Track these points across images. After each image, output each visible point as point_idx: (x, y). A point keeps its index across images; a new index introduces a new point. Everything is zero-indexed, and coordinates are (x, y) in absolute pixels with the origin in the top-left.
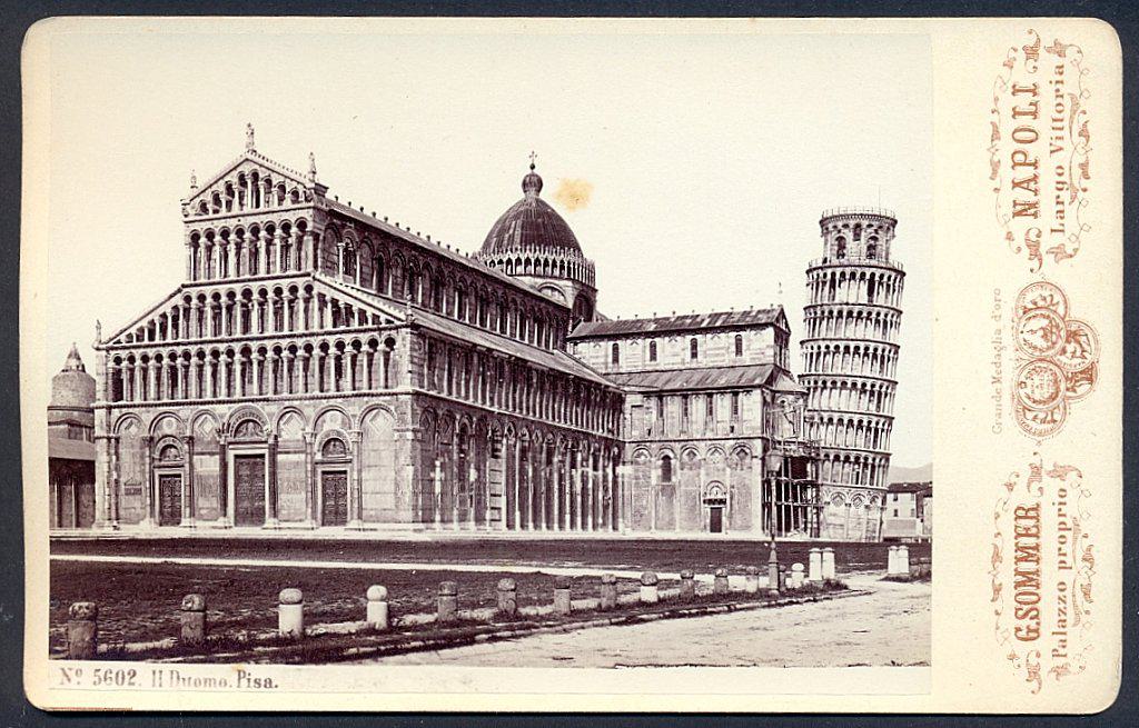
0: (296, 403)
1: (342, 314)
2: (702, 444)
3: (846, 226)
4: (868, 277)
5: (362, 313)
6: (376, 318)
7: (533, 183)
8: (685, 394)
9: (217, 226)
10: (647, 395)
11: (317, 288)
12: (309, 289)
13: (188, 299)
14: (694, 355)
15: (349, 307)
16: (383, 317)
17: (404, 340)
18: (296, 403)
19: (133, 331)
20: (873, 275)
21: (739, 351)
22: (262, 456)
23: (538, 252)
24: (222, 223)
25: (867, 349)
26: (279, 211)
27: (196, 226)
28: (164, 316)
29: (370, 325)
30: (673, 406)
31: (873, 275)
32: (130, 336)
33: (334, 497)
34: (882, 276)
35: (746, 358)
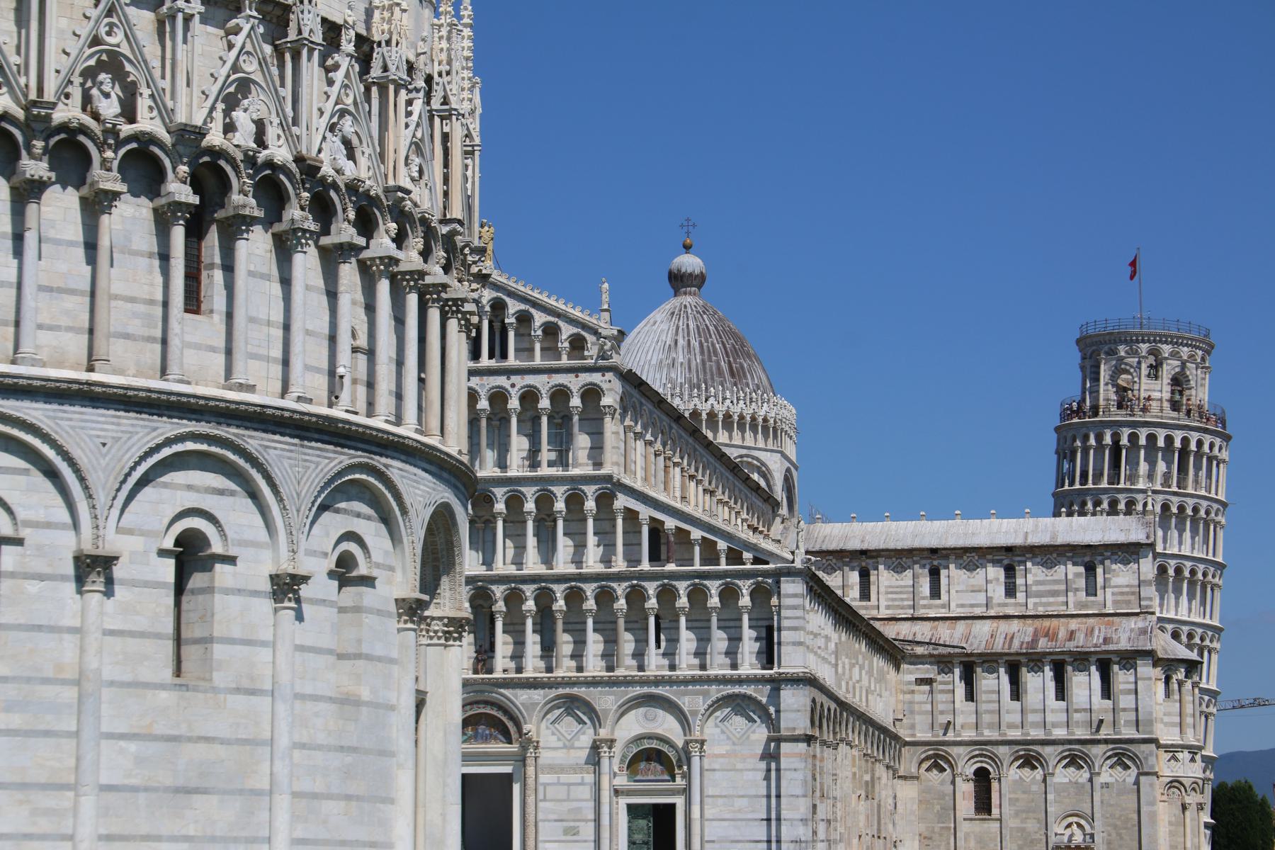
0: (575, 691)
2: (1047, 751)
3: (1134, 353)
4: (1178, 444)
5: (708, 546)
8: (1015, 666)
10: (944, 663)
11: (622, 501)
12: (605, 500)
14: (1011, 591)
15: (682, 534)
16: (747, 556)
18: (575, 691)
20: (1185, 441)
21: (1091, 590)
23: (712, 400)
25: (1178, 571)
29: (723, 566)
30: (993, 683)
31: (1185, 441)
34: (1200, 443)
35: (1108, 600)
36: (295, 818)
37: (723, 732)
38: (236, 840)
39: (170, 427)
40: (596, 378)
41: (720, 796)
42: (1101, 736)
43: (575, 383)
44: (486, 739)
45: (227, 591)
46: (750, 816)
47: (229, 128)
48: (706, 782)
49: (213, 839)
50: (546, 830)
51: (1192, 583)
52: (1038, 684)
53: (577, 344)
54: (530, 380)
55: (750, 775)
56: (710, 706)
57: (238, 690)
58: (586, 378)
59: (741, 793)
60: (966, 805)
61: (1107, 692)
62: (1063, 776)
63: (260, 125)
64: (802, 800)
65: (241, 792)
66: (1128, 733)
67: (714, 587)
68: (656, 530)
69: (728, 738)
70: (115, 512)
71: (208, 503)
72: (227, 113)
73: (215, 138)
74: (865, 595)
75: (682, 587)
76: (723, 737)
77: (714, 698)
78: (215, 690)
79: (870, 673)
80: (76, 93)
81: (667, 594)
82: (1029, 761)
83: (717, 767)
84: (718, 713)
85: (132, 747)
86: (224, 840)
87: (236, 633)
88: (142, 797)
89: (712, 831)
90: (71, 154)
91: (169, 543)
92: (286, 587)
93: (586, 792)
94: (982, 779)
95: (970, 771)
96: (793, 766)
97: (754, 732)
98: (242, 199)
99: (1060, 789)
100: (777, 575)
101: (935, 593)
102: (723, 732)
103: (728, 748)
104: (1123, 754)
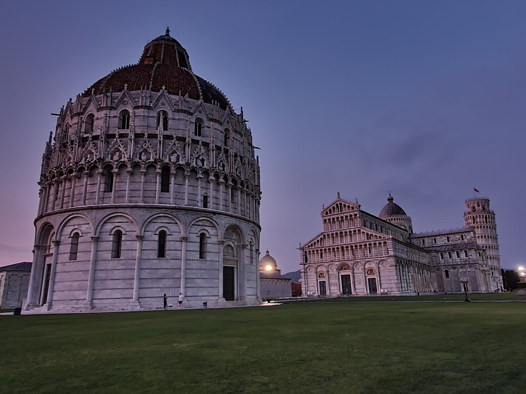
1: (369, 236)
6: (380, 237)
7: (391, 200)
9: (331, 217)
13: (324, 236)
14: (448, 241)
17: (390, 242)
19: (310, 244)
20: (486, 216)
21: (463, 239)
22: (349, 275)
24: (333, 217)
26: (346, 212)
27: (325, 218)
28: (318, 241)
32: (309, 247)
33: (372, 285)
36: (186, 283)
38: (172, 288)
39: (155, 212)
40: (356, 212)
42: (467, 263)
43: (353, 214)
44: (346, 269)
45: (170, 241)
47: (170, 160)
49: (166, 287)
50: (356, 283)
51: (491, 238)
52: (454, 255)
53: (353, 208)
54: (347, 214)
57: (172, 259)
58: (354, 213)
60: (444, 276)
61: (467, 256)
62: (461, 270)
63: (178, 158)
65: (173, 278)
66: (472, 262)
67: (377, 242)
68: (368, 234)
70: (144, 228)
71: (166, 225)
72: (169, 157)
73: (167, 161)
74: (424, 244)
75: (372, 243)
78: (167, 259)
79: (419, 255)
80: (138, 156)
81: (370, 244)
82: (454, 268)
85: (148, 271)
86: (169, 287)
87: (172, 249)
88: (150, 280)
89: (382, 282)
90: (136, 165)
91: (157, 233)
92: (185, 239)
93: (361, 277)
94: (447, 272)
95: (444, 270)
98: (173, 170)
99: (460, 272)
100: (387, 239)
101: (435, 242)
104: (471, 265)
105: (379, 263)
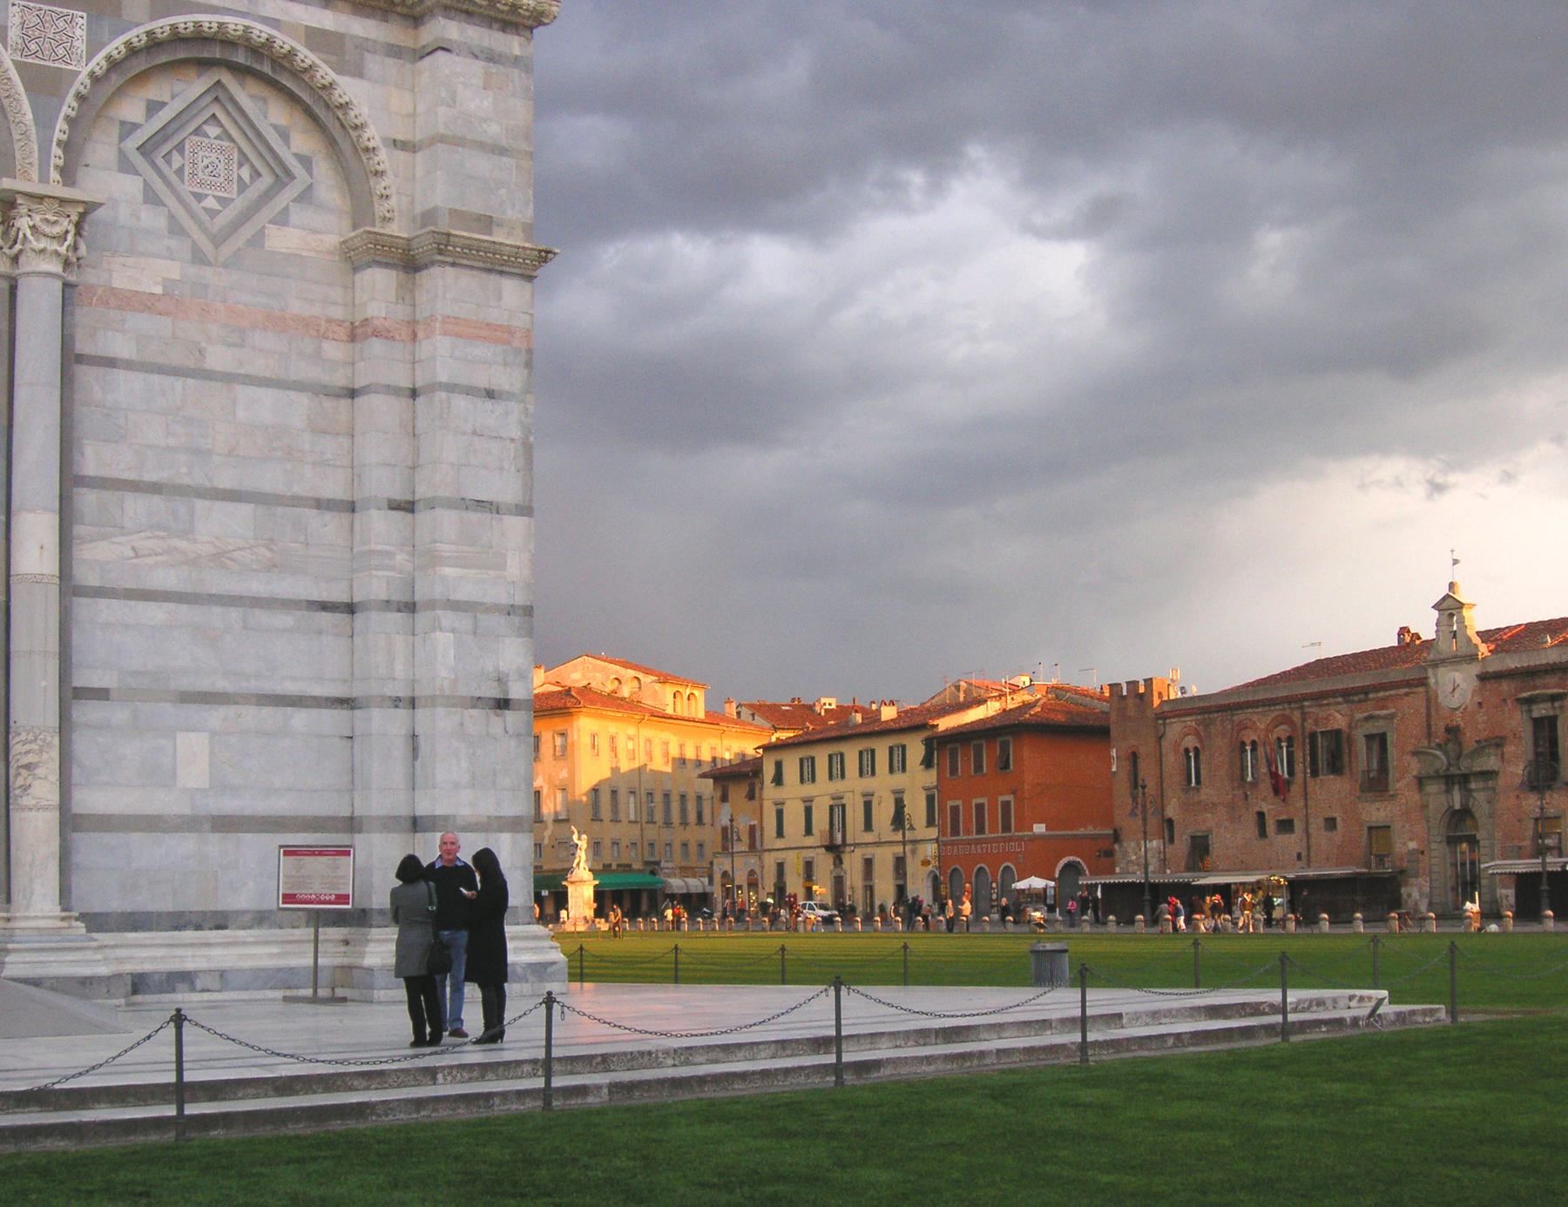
37: (151, 197)
41: (135, 487)
46: (257, 586)
48: (88, 420)
55: (261, 406)
56: (114, 65)
59: (224, 481)
64: (515, 526)
69: (175, 228)
76: (151, 219)
77: (137, 35)
83: (121, 347)
84: (131, 109)
96: (482, 380)
97: (282, 219)
102: (151, 197)
103: (174, 271)
105: (92, 109)
